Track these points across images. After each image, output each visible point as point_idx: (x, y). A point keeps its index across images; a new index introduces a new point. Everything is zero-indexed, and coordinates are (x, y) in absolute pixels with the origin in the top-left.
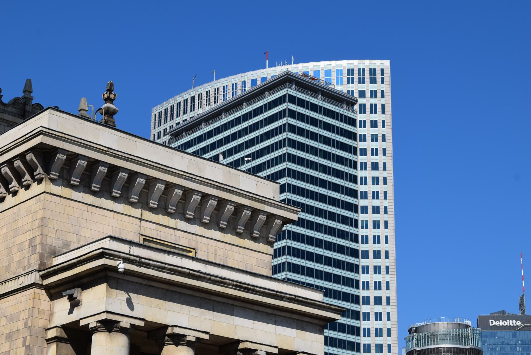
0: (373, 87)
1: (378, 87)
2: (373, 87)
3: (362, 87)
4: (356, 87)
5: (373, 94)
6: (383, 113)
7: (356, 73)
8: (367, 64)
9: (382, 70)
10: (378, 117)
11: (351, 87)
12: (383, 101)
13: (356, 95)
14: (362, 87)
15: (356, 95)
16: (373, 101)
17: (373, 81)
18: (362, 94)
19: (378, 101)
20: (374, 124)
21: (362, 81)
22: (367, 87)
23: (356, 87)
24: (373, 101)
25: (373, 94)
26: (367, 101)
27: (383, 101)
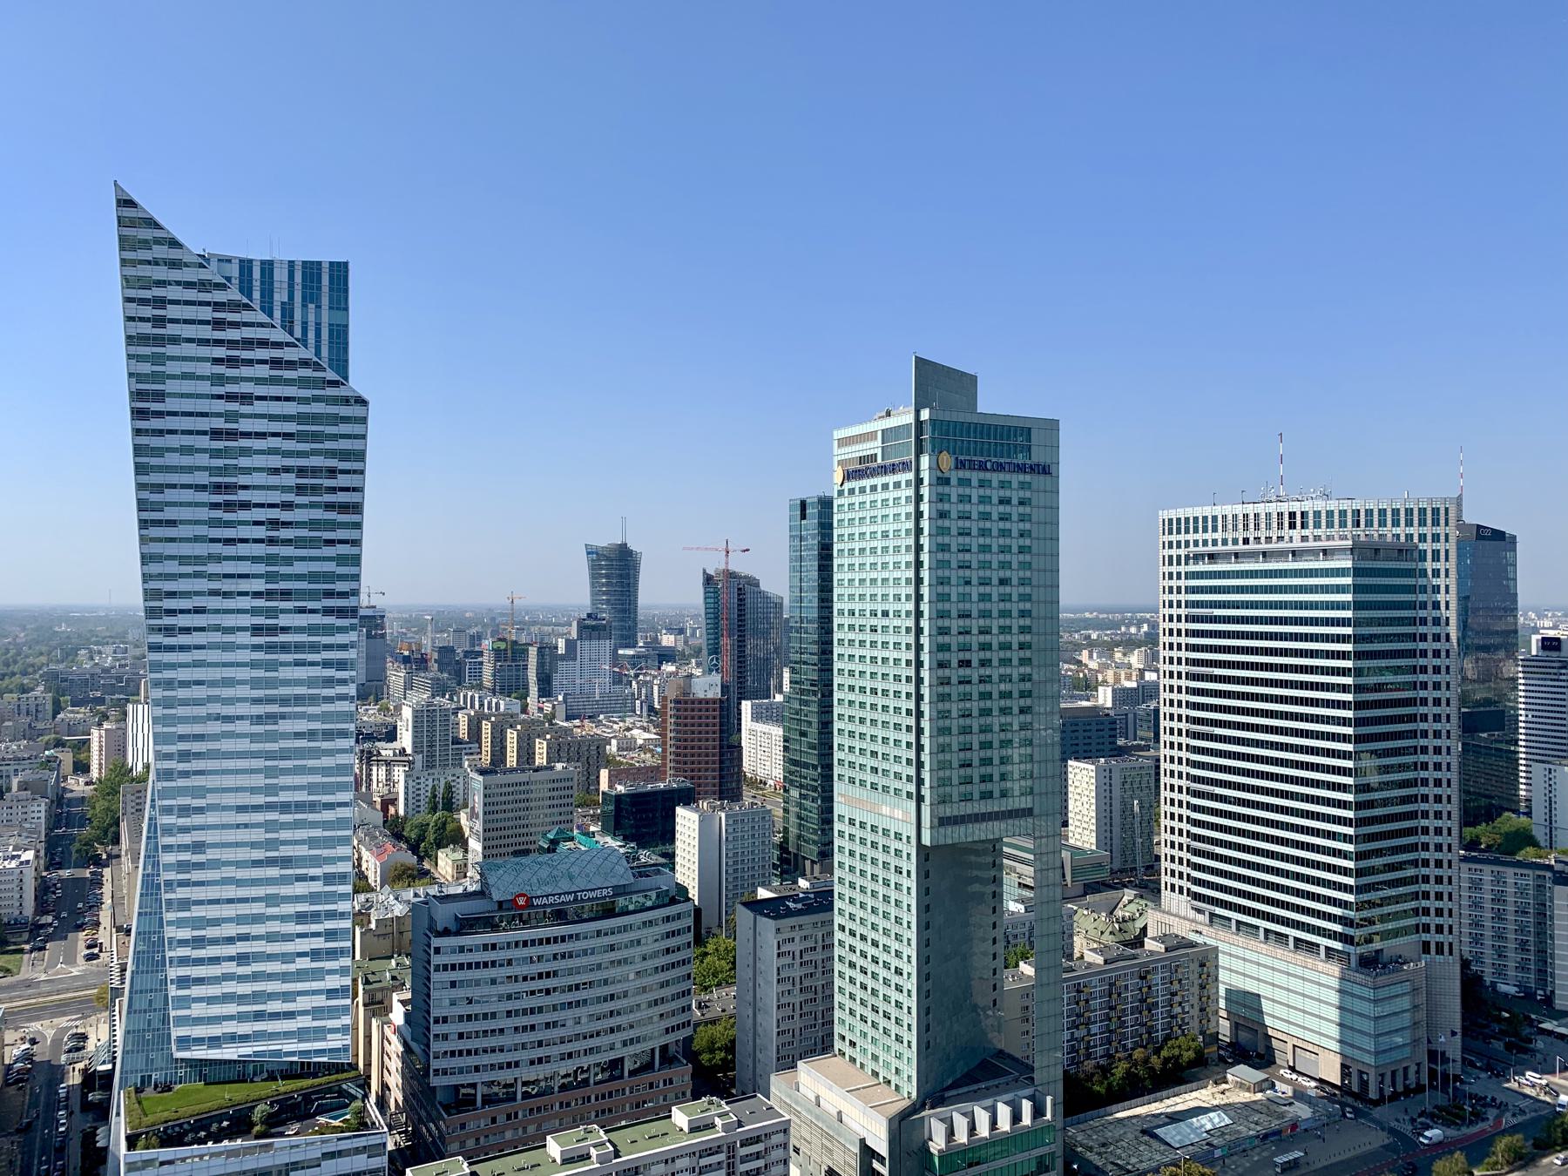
4: (1414, 531)
13: (1416, 540)
15: (1416, 540)
22: (1428, 530)
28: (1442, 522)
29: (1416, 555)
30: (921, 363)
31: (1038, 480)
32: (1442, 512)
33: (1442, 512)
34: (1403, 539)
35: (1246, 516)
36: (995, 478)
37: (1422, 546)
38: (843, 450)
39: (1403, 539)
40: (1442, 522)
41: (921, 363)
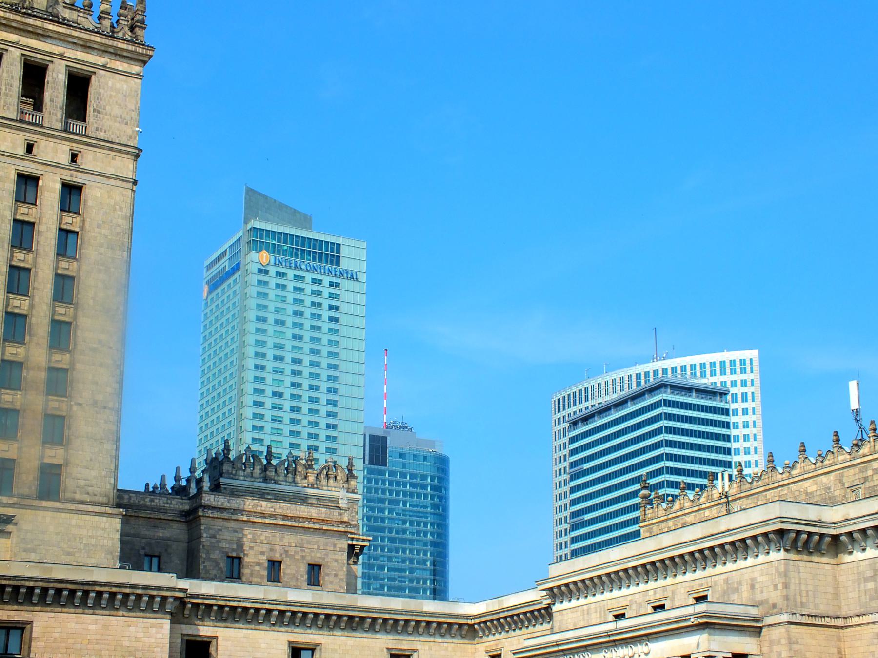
0: (744, 377)
1: (747, 377)
2: (744, 377)
3: (733, 377)
4: (728, 378)
5: (744, 383)
6: (753, 400)
7: (728, 364)
8: (737, 355)
9: (751, 360)
10: (749, 405)
11: (723, 378)
12: (752, 389)
14: (733, 377)
15: (729, 385)
16: (744, 390)
17: (743, 371)
18: (734, 384)
19: (748, 390)
20: (745, 412)
21: (733, 372)
23: (728, 378)
24: (744, 390)
25: (744, 383)
26: (738, 390)
27: (752, 389)
28: (748, 370)
29: (729, 397)
30: (250, 192)
31: (345, 284)
32: (748, 362)
33: (748, 362)
34: (719, 385)
35: (606, 383)
36: (309, 277)
37: (733, 390)
38: (210, 272)
39: (719, 385)
40: (748, 370)
41: (250, 192)
